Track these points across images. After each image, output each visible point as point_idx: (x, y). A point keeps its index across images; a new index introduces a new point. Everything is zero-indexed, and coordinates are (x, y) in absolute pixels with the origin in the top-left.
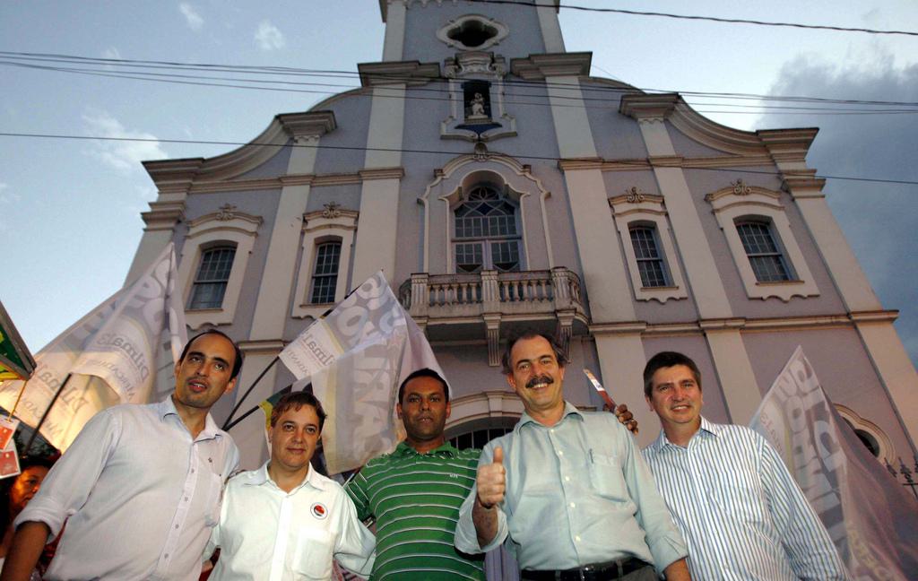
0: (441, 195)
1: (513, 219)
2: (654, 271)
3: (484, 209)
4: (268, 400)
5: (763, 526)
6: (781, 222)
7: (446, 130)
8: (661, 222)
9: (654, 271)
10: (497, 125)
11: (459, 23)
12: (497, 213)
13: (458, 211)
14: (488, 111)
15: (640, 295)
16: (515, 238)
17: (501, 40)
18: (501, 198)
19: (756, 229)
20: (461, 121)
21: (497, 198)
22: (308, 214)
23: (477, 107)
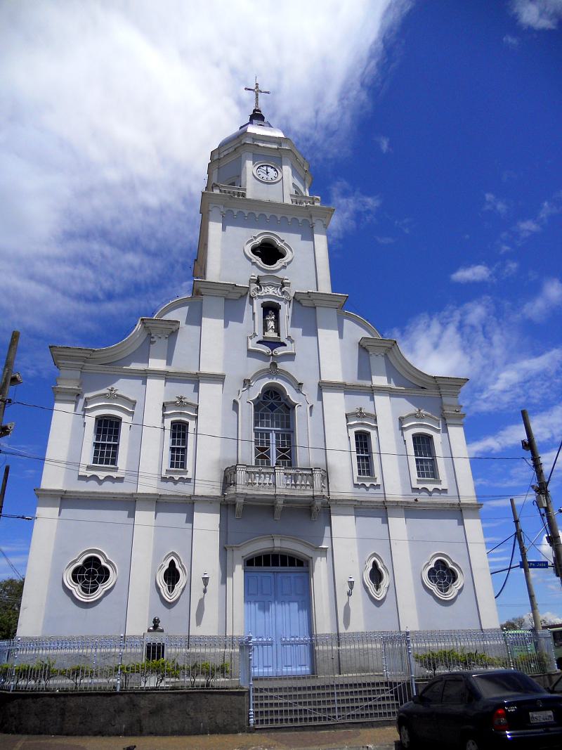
0: (249, 398)
1: (289, 416)
2: (365, 463)
3: (272, 408)
4: (21, 585)
5: (430, 664)
6: (438, 439)
7: (252, 345)
8: (373, 433)
9: (365, 463)
10: (284, 344)
11: (259, 241)
12: (280, 411)
13: (257, 407)
14: (277, 330)
15: (415, 485)
16: (289, 432)
17: (289, 263)
18: (282, 401)
19: (423, 444)
20: (260, 338)
21: (280, 400)
22: (167, 403)
23: (271, 324)
